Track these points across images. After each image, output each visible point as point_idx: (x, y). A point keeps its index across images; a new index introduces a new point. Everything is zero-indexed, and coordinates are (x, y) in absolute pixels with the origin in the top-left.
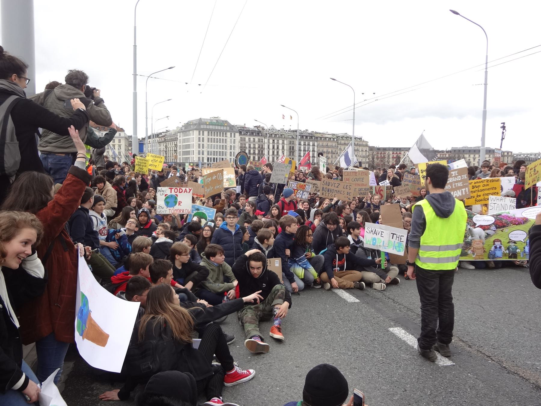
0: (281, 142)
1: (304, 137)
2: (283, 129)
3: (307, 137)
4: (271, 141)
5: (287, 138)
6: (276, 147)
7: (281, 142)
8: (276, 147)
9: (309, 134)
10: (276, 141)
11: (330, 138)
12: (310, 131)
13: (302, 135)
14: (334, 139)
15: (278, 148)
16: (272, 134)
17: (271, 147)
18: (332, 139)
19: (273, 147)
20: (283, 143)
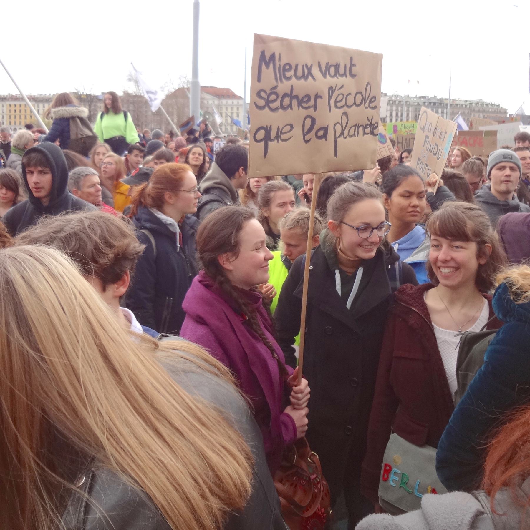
0: (405, 109)
1: (432, 104)
2: (408, 95)
3: (435, 103)
4: (394, 108)
5: (412, 106)
6: (399, 115)
7: (405, 109)
8: (399, 115)
9: (438, 100)
10: (400, 108)
11: (462, 105)
12: (438, 98)
13: (430, 101)
14: (466, 106)
15: (402, 115)
16: (395, 101)
17: (394, 114)
18: (464, 106)
19: (397, 115)
20: (408, 111)
